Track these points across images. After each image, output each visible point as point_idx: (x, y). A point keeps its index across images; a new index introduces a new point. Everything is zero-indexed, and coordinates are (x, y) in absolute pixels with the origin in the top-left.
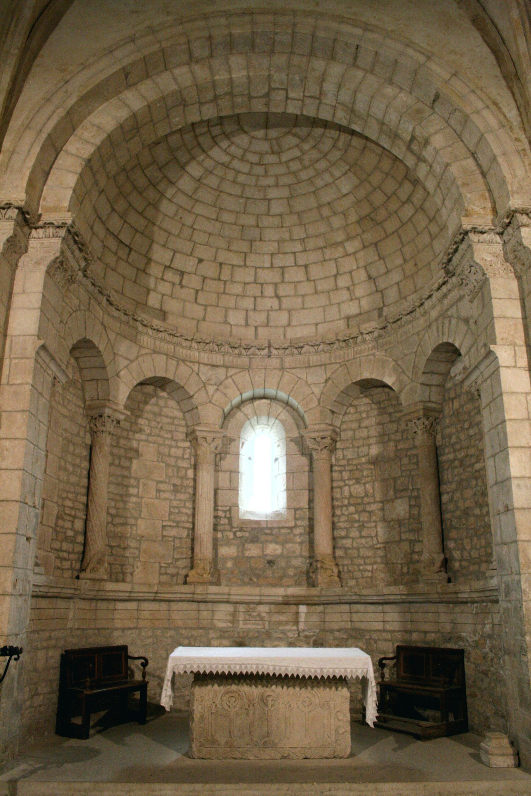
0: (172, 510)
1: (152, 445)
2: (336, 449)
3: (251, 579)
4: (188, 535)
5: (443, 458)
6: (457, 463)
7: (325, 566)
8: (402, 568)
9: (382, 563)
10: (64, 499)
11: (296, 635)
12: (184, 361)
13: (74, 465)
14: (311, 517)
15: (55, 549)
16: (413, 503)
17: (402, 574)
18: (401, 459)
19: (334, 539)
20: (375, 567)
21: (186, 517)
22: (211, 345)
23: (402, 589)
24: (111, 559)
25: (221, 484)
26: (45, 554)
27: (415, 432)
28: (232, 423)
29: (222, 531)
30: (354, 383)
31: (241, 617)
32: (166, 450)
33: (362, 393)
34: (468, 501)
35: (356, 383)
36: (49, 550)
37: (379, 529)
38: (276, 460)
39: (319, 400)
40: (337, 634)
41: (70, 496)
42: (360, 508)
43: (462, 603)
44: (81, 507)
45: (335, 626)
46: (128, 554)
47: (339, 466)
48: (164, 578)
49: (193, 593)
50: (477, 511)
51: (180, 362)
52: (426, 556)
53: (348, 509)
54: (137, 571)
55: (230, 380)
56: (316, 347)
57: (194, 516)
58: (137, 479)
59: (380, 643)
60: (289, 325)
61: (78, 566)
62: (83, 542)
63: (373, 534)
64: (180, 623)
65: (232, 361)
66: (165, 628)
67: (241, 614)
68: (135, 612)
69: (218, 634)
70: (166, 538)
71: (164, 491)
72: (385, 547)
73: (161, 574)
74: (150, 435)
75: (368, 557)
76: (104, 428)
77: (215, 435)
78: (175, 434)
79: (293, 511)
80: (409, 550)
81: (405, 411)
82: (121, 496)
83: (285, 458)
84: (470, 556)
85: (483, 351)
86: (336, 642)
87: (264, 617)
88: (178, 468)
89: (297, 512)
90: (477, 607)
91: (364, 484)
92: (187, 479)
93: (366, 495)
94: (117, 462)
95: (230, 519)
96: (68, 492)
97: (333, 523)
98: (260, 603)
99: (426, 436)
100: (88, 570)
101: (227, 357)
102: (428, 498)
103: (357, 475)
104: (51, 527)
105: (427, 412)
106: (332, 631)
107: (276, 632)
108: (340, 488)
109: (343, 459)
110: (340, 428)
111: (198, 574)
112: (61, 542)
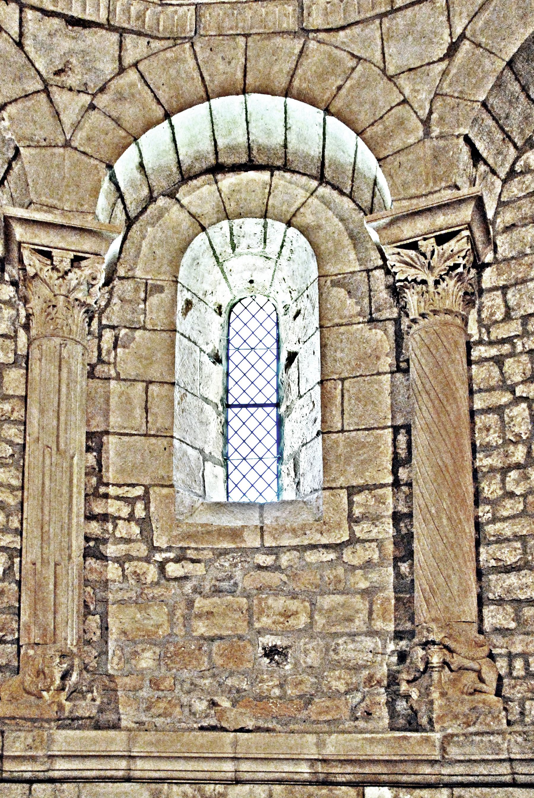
3: (213, 704)
29: (120, 561)
47: (491, 343)
79: (344, 494)
89: (356, 498)
98: (238, 782)
108: (499, 410)
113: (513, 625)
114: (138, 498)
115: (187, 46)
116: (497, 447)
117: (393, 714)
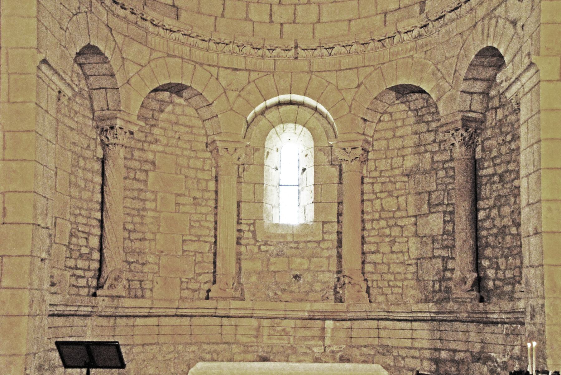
0: (192, 224)
1: (169, 156)
2: (368, 160)
3: (276, 294)
4: (210, 250)
5: (481, 173)
6: (496, 178)
7: (353, 282)
8: (433, 286)
9: (412, 279)
10: (76, 216)
11: (323, 351)
12: (201, 64)
13: (86, 180)
14: (339, 230)
15: (70, 268)
16: (448, 218)
17: (434, 291)
18: (437, 171)
19: (363, 253)
20: (406, 283)
21: (208, 231)
22: (231, 45)
23: (432, 307)
24: (130, 276)
25: (244, 197)
26: (60, 272)
27: (453, 144)
28: (255, 130)
29: (246, 245)
30: (388, 89)
31: (266, 331)
32: (184, 162)
33: (397, 99)
34: (505, 220)
35: (392, 89)
36: (64, 268)
37: (410, 245)
38: (304, 170)
39: (350, 107)
40: (364, 349)
41: (84, 212)
42: (391, 222)
43: (493, 323)
44: (96, 223)
45: (362, 342)
46: (146, 270)
47: (370, 177)
48: (186, 293)
49: (216, 308)
50: (514, 230)
51: (197, 66)
52: (457, 274)
53: (379, 223)
54: (157, 286)
55: (252, 85)
56: (348, 48)
57: (216, 229)
58: (155, 193)
59: (407, 360)
60: (319, 21)
61: (94, 283)
62: (99, 259)
63: (405, 250)
64: (203, 339)
65: (255, 64)
66: (187, 344)
67: (266, 329)
68: (156, 328)
69: (242, 348)
70: (187, 253)
71: (183, 205)
72: (417, 264)
73: (183, 289)
74: (167, 145)
75: (398, 273)
76: (115, 141)
77: (238, 145)
78: (194, 144)
79: (321, 224)
80: (441, 268)
81: (443, 121)
82: (138, 210)
83: (313, 168)
84: (505, 276)
85: (526, 61)
86: (363, 358)
87: (289, 332)
88: (198, 181)
89: (325, 226)
90: (507, 329)
91: (397, 197)
92: (209, 191)
93: (399, 209)
94: (132, 175)
95: (254, 233)
96: (81, 209)
97: (363, 237)
99: (463, 149)
100: (105, 287)
101: (249, 59)
102: (463, 214)
103: (390, 187)
104: (65, 245)
105: (466, 122)
106: (359, 347)
107: (301, 347)
108: (371, 200)
109: (376, 169)
110: (372, 137)
111: (221, 289)
112: (76, 259)
113: (374, 271)
114: (252, 224)
115: (272, 75)
116: (371, 213)
117: (336, 298)
